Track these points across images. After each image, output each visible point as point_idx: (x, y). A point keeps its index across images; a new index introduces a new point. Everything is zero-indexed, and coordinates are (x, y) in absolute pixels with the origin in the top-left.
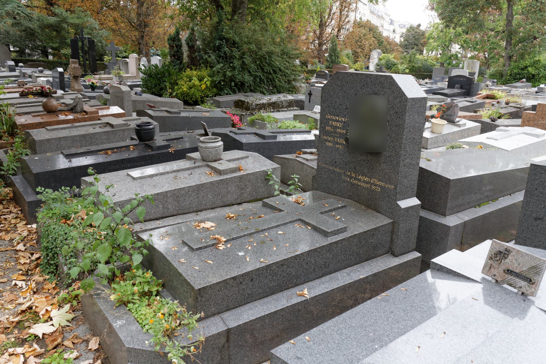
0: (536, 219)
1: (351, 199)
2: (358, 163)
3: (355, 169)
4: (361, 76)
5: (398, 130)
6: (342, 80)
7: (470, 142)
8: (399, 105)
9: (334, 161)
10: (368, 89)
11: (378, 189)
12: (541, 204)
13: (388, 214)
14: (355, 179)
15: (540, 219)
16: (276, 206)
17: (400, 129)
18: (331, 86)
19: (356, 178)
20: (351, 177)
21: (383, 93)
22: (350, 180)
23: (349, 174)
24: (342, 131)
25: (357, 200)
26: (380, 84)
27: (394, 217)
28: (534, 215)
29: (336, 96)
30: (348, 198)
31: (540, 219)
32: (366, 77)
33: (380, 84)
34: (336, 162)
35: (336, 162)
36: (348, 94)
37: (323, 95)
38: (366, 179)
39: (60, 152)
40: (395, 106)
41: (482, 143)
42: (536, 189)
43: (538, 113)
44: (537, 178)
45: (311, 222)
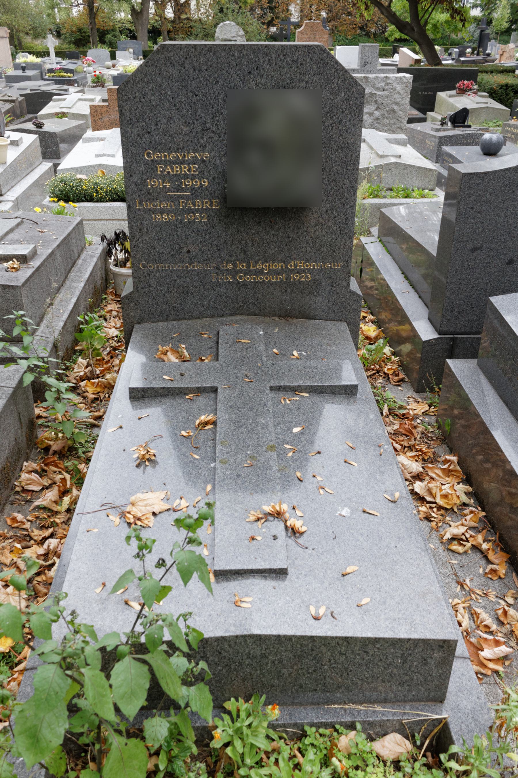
0: (473, 250)
1: (242, 314)
2: (253, 241)
3: (245, 252)
4: (240, 52)
5: (346, 156)
6: (183, 65)
7: (80, 167)
8: (344, 106)
9: (185, 250)
10: (263, 81)
11: (307, 277)
12: (478, 228)
13: (333, 315)
14: (248, 272)
15: (478, 249)
16: (169, 385)
17: (350, 153)
18: (147, 83)
19: (250, 271)
20: (235, 272)
21: (303, 84)
22: (234, 277)
23: (230, 266)
24: (196, 183)
25: (257, 312)
26: (294, 66)
27: (347, 316)
28: (470, 246)
29: (167, 105)
30: (233, 315)
31: (478, 249)
32: (254, 52)
33: (294, 66)
34: (189, 252)
35: (189, 252)
36: (205, 95)
37: (127, 107)
38: (278, 266)
39: (142, 601)
40: (334, 109)
41: (100, 165)
42: (472, 208)
43: (112, 104)
44: (472, 192)
45: (301, 383)
